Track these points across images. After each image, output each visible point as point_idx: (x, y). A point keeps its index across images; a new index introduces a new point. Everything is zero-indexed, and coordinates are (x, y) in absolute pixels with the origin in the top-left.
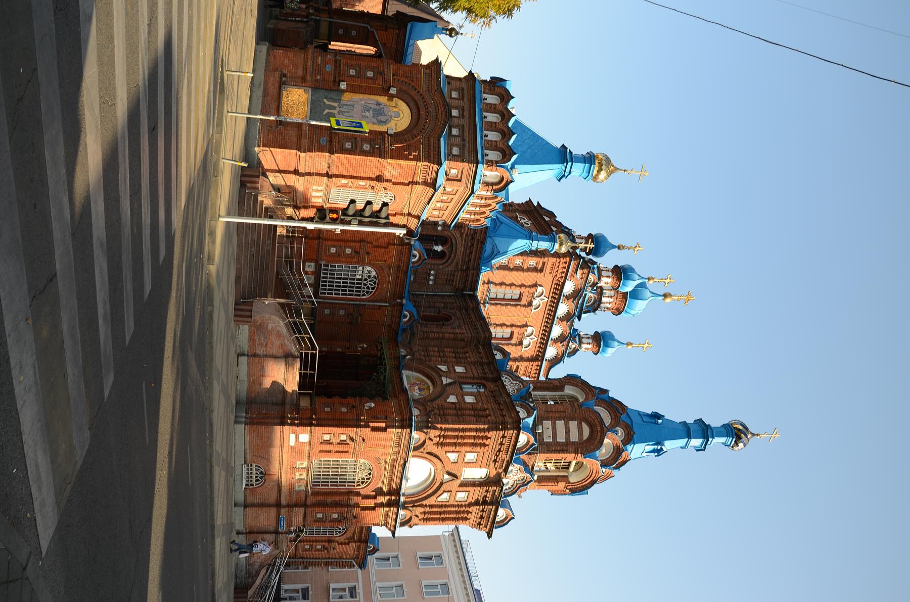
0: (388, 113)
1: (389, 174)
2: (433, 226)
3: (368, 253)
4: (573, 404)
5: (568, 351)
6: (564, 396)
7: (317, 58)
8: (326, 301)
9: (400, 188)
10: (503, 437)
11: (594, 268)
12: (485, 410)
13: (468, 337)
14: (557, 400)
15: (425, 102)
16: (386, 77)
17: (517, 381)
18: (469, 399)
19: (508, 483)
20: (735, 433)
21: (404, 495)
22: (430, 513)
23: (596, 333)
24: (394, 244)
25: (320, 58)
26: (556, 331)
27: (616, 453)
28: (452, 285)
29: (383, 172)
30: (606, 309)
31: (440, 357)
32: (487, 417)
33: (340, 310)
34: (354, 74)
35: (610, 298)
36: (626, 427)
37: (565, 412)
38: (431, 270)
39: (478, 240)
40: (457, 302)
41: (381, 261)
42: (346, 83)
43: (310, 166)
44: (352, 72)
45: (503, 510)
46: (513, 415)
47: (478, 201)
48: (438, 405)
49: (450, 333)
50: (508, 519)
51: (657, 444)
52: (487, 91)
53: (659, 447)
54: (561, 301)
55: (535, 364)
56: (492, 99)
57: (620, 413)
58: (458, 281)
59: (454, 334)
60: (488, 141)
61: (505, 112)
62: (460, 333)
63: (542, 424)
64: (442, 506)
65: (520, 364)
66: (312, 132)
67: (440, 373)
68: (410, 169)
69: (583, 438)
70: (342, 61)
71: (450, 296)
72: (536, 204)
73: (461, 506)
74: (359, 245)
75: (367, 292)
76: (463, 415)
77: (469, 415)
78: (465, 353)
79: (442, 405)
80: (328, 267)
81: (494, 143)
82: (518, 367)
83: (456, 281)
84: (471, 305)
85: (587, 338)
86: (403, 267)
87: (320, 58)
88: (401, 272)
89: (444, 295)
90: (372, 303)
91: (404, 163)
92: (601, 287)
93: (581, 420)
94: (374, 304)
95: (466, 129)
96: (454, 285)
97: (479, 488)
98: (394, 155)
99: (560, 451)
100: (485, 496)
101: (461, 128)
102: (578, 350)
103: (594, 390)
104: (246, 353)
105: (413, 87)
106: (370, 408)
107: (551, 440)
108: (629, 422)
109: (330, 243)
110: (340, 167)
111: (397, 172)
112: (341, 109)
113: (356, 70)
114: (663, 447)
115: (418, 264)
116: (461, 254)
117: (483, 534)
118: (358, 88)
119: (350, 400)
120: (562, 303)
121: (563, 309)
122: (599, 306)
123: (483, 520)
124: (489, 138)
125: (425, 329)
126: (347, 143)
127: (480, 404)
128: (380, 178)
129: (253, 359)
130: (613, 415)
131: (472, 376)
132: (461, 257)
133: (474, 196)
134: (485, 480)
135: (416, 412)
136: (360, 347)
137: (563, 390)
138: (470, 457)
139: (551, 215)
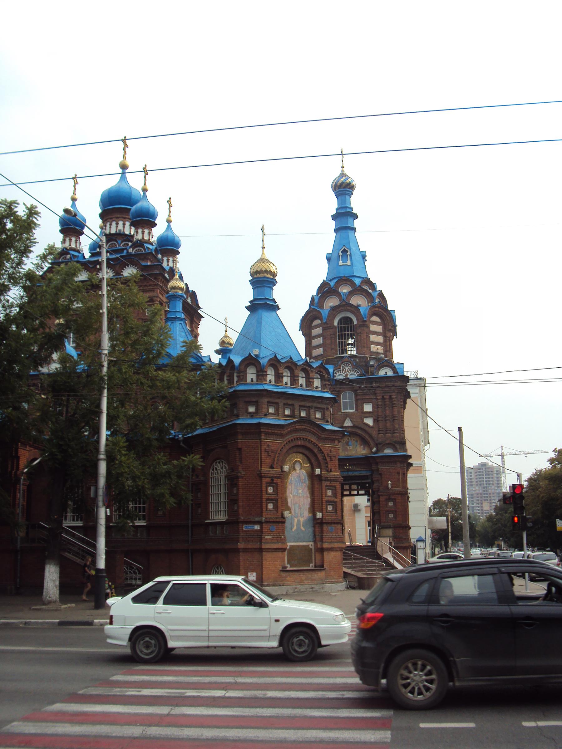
7: (267, 539)
15: (294, 439)
16: (276, 475)
25: (266, 537)
35: (126, 226)
70: (265, 516)
87: (266, 537)
95: (303, 403)
102: (181, 274)
130: (358, 293)
135: (388, 452)
136: (24, 469)
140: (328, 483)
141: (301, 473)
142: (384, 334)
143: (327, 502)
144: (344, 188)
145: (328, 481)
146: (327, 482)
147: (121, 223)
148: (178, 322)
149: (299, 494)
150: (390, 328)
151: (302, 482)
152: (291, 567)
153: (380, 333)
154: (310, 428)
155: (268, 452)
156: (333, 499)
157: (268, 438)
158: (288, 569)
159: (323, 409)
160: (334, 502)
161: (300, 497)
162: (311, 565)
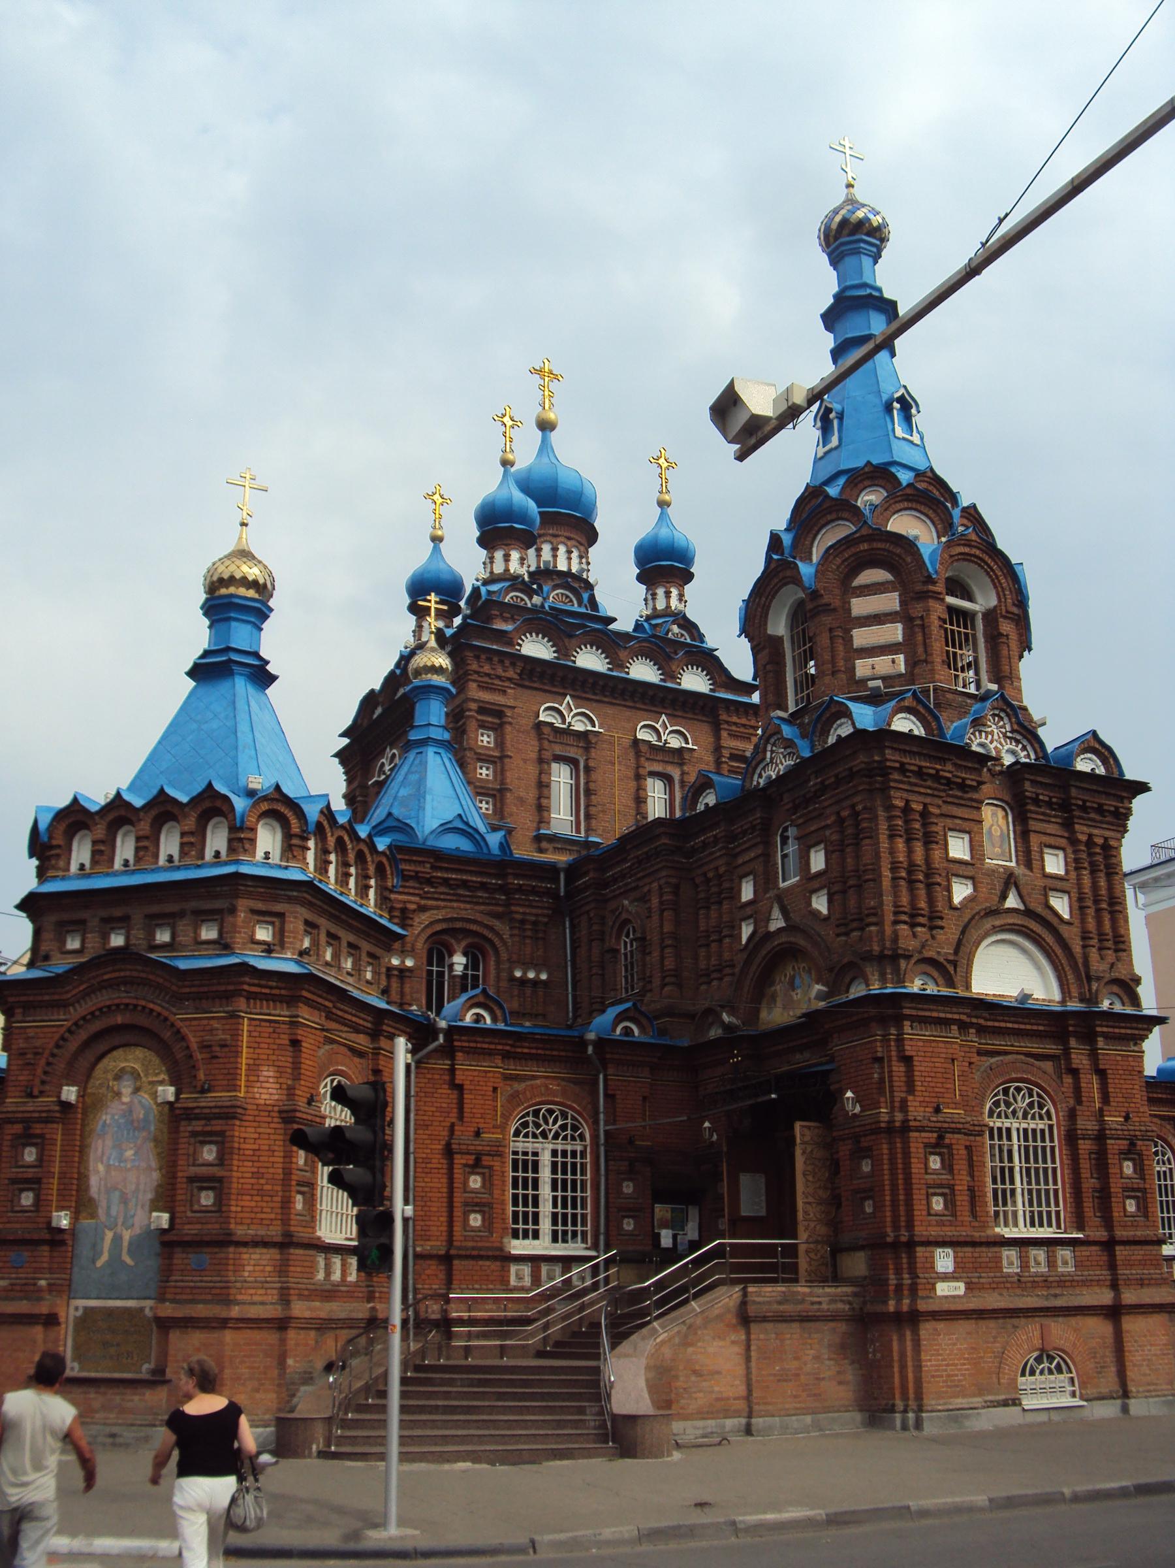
0: (124, 1104)
1: (274, 1091)
2: (407, 980)
3: (478, 1134)
4: (811, 611)
5: (689, 641)
6: (792, 637)
8: (602, 1229)
9: (308, 1062)
10: (902, 769)
11: (489, 592)
12: (841, 821)
13: (669, 876)
14: (805, 651)
16: (36, 1115)
17: (765, 751)
18: (818, 861)
19: (1013, 753)
20: (850, 235)
21: (1063, 1002)
22: (1101, 935)
23: (640, 578)
24: (452, 1071)
26: (643, 671)
27: (918, 502)
28: (546, 924)
29: (270, 1108)
30: (584, 560)
31: (720, 941)
32: (857, 814)
33: (622, 1193)
34: (31, 1195)
36: (856, 485)
37: (831, 630)
38: (513, 979)
39: (433, 867)
40: (587, 908)
41: (495, 1100)
42: (55, 1214)
43: (262, 1291)
44: (27, 1199)
45: (1079, 759)
46: (848, 752)
47: (332, 869)
48: (838, 935)
49: (661, 919)
50: (1097, 746)
51: (889, 408)
52: (61, 864)
53: (896, 405)
54: (570, 664)
55: (724, 716)
56: (81, 853)
57: (823, 501)
58: (534, 911)
59: (662, 911)
60: (183, 853)
61: (111, 816)
62: (661, 896)
63: (864, 681)
64: (1081, 908)
65: (726, 753)
66: (179, 1290)
67: (761, 938)
68: (258, 1040)
69: (888, 582)
71: (573, 926)
72: (346, 741)
73: (1076, 860)
74: (458, 1156)
75: (575, 1128)
76: (857, 871)
77: (857, 857)
78: (708, 880)
79: (837, 926)
80: (518, 1229)
81: (186, 839)
82: (733, 757)
83: (537, 915)
84: (591, 875)
85: (654, 599)
86: (506, 1044)
88: (519, 1050)
89: (573, 941)
90: (602, 1116)
91: (244, 1055)
92: (531, 574)
93: (849, 591)
94: (602, 1109)
95: (155, 909)
96: (546, 920)
97: (1031, 822)
98: (225, 1082)
99: (924, 634)
100: (1049, 804)
101: (155, 920)
103: (773, 565)
104: (743, 1421)
105: (58, 1046)
106: (857, 1100)
107: (902, 657)
108: (841, 481)
109: (457, 1228)
110: (263, 1216)
111: (267, 1073)
112: (120, 1221)
113: (22, 1190)
114: (896, 395)
115: (495, 1008)
116: (468, 906)
117: (1139, 803)
118: (66, 1181)
119: (841, 1154)
120: (574, 662)
121: (590, 660)
122: (577, 578)
123: (1106, 807)
124: (175, 851)
125: (657, 982)
126: (204, 1202)
127: (828, 833)
128: (284, 1115)
129: (758, 1404)
130: (829, 517)
131: (761, 859)
132: (476, 907)
133: (321, 881)
134: (1012, 809)
136: (712, 1136)
137: (780, 639)
138: (958, 848)
139: (370, 701)
140: (197, 1126)
141: (136, 1101)
142: (903, 616)
143: (191, 1180)
144: (836, 238)
145: (199, 1119)
146: (194, 1123)
147: (546, 549)
148: (430, 751)
149: (126, 1161)
150: (919, 587)
151: (135, 1129)
152: (81, 1369)
153: (896, 613)
154: (143, 975)
155: (210, 1046)
156: (216, 1171)
157: (273, 1012)
158: (68, 1373)
159: (220, 912)
160: (220, 1180)
161: (129, 1170)
162: (146, 1366)
